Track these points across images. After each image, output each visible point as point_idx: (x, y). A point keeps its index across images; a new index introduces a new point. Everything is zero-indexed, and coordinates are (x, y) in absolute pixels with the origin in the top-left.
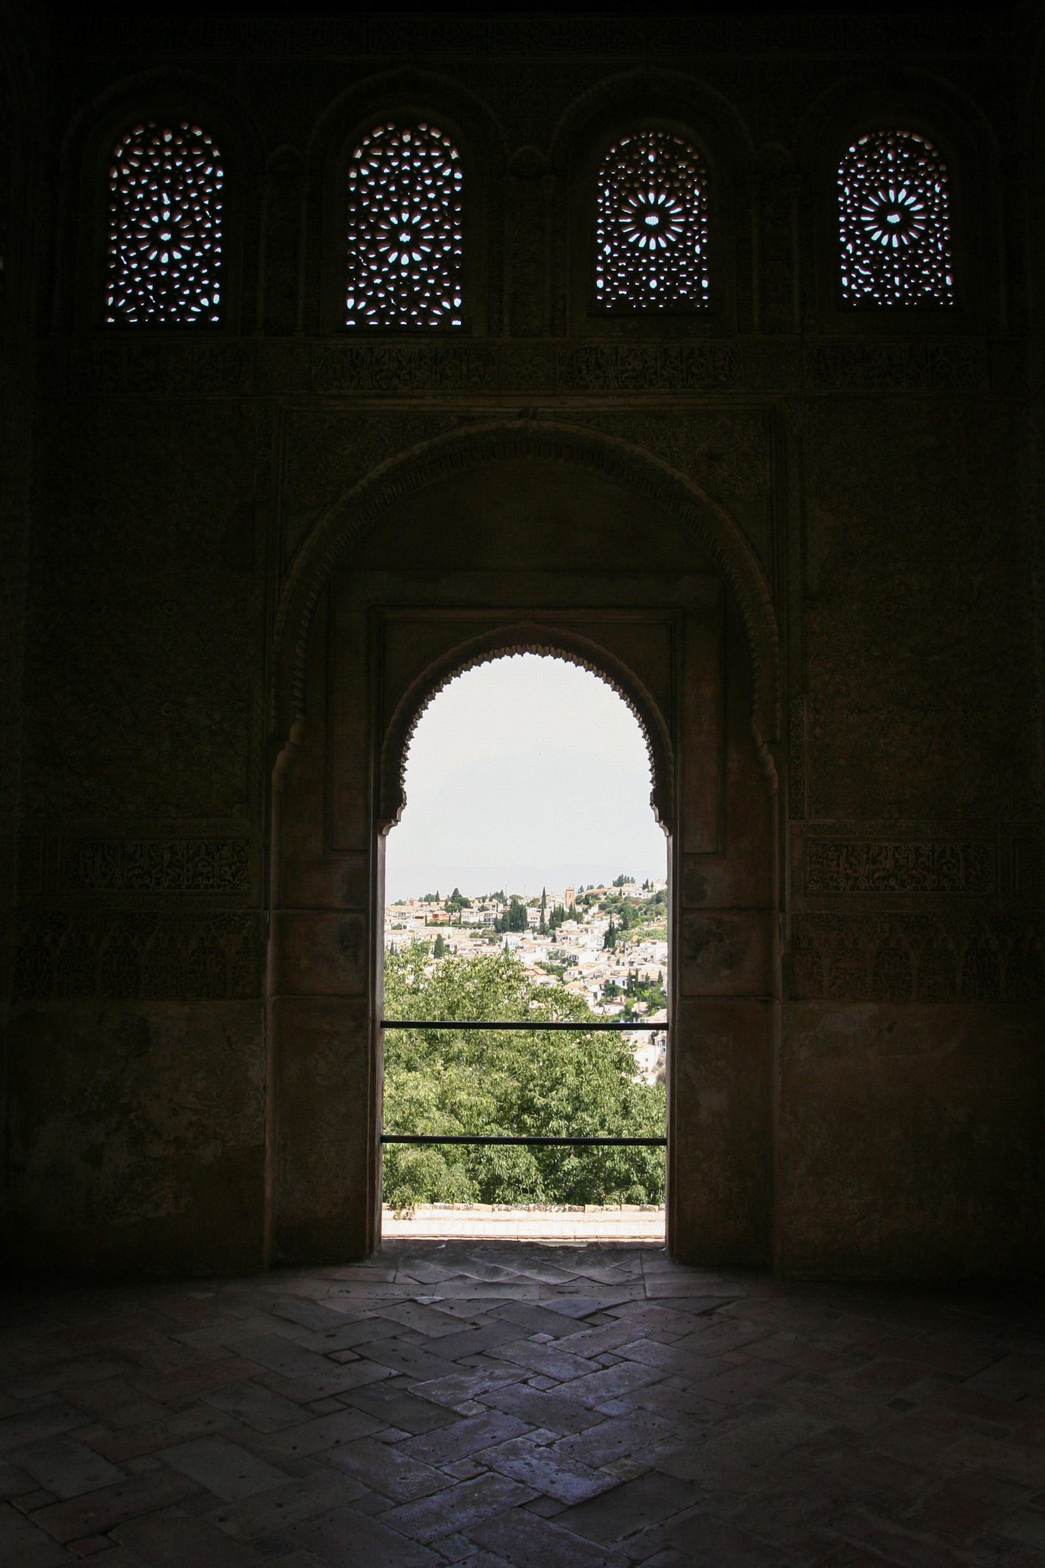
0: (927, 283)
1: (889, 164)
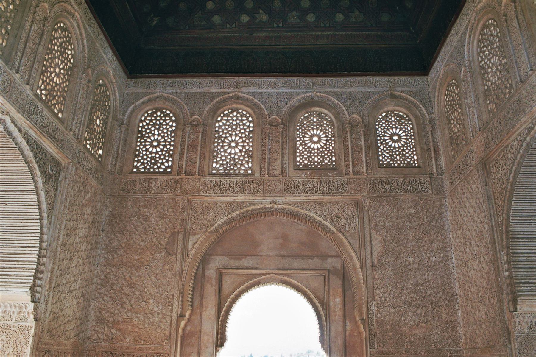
0: (408, 158)
1: (393, 121)
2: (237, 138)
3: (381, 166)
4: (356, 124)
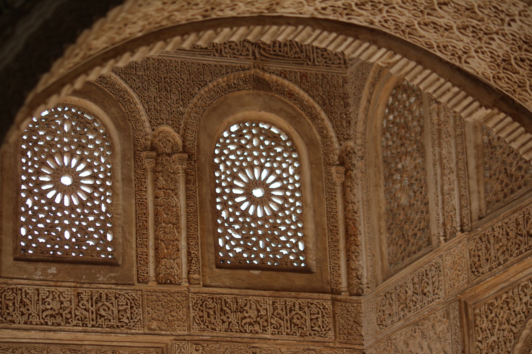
0: (284, 247)
3: (221, 264)
4: (169, 151)
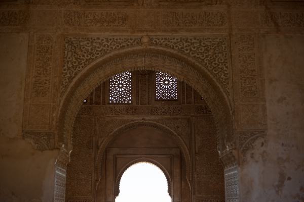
2: (123, 82)
